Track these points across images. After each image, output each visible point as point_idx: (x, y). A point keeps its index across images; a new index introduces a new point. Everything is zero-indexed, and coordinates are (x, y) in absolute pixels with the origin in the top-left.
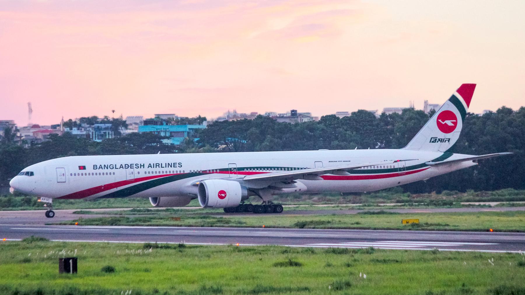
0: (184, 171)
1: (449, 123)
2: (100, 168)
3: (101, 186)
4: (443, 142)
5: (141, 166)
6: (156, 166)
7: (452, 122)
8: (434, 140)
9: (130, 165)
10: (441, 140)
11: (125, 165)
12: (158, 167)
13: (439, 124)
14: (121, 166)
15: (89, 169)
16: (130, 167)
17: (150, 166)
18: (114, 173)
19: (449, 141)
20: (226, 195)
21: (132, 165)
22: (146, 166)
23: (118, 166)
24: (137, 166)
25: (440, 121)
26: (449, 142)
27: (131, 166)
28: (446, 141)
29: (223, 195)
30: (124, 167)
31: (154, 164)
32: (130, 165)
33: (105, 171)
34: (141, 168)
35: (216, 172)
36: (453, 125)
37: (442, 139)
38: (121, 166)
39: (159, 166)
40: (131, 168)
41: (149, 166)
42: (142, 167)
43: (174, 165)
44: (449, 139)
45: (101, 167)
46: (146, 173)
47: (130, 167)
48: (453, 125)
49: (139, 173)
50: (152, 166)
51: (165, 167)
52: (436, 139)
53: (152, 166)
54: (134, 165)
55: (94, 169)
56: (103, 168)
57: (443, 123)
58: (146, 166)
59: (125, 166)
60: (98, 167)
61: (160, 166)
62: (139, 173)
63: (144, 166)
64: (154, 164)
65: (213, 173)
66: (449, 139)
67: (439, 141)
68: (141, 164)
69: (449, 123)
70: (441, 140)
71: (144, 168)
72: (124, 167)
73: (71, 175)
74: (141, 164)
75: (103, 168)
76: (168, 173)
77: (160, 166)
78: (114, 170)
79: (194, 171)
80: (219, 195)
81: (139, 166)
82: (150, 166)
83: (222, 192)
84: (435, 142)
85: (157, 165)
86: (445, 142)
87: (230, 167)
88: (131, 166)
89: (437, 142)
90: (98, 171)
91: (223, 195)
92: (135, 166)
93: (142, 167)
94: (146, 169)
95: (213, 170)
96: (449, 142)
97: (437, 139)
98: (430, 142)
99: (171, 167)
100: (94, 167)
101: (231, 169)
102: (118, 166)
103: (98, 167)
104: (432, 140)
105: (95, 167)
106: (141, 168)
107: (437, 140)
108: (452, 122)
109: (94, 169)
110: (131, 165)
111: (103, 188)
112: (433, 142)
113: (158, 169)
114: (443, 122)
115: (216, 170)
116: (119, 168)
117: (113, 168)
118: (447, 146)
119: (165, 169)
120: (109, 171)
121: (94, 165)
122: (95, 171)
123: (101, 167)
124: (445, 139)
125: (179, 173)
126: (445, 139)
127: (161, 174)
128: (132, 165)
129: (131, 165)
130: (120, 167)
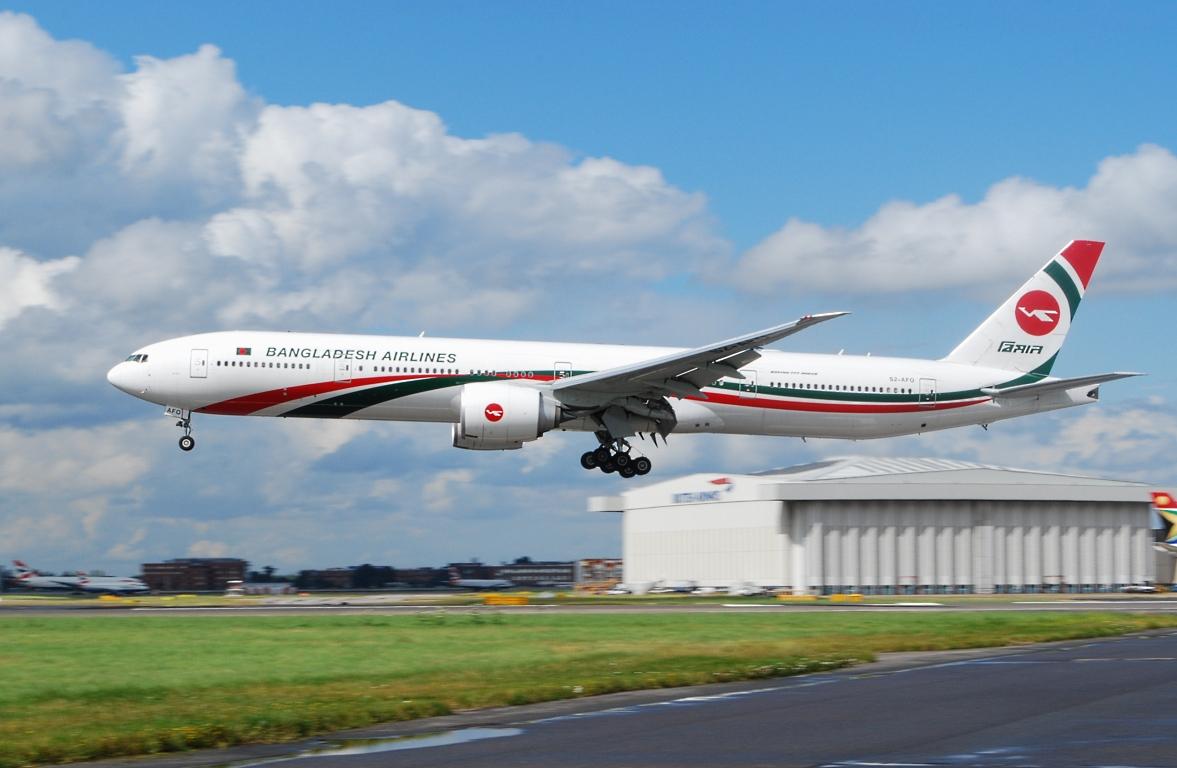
1: (1042, 315)
3: (281, 391)
7: (1048, 314)
8: (1008, 347)
10: (1024, 349)
12: (403, 359)
13: (1020, 316)
14: (327, 353)
17: (387, 356)
22: (379, 356)
24: (360, 355)
25: (1023, 309)
30: (332, 354)
32: (345, 352)
33: (291, 360)
35: (527, 378)
36: (1051, 320)
37: (1025, 347)
44: (1041, 348)
45: (283, 352)
46: (376, 369)
48: (1051, 320)
49: (361, 368)
50: (392, 357)
52: (1012, 346)
53: (392, 358)
57: (1030, 315)
58: (379, 356)
60: (277, 352)
61: (409, 357)
62: (361, 368)
65: (520, 377)
69: (1042, 315)
70: (1024, 349)
72: (332, 355)
73: (219, 363)
75: (288, 354)
76: (424, 373)
77: (409, 357)
81: (365, 355)
85: (403, 355)
87: (557, 369)
88: (347, 354)
89: (1015, 351)
90: (275, 360)
93: (370, 357)
94: (378, 362)
103: (277, 352)
104: (1004, 347)
105: (271, 352)
107: (1015, 347)
108: (1048, 314)
111: (285, 394)
112: (1005, 350)
114: (1030, 311)
118: (1038, 360)
119: (417, 365)
123: (283, 352)
125: (446, 373)
127: (409, 373)
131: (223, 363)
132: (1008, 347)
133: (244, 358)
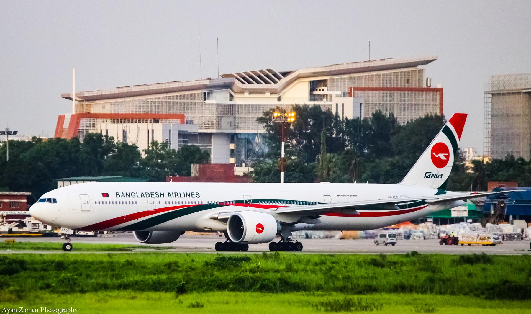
0: (202, 202)
2: (122, 196)
4: (436, 178)
5: (161, 195)
6: (175, 195)
8: (428, 175)
9: (150, 194)
10: (435, 176)
11: (146, 193)
14: (142, 195)
15: (112, 197)
16: (150, 196)
18: (136, 203)
19: (441, 176)
20: (263, 229)
21: (152, 194)
23: (139, 195)
26: (441, 178)
27: (151, 194)
28: (439, 176)
29: (261, 229)
31: (173, 193)
32: (150, 194)
33: (128, 199)
34: (161, 197)
37: (435, 174)
38: (142, 195)
39: (177, 195)
40: (152, 197)
41: (168, 196)
42: (162, 196)
43: (192, 195)
44: (442, 174)
45: (123, 195)
47: (150, 196)
51: (184, 196)
52: (430, 174)
54: (154, 194)
55: (117, 197)
56: (125, 196)
58: (166, 195)
59: (146, 195)
60: (121, 195)
61: (179, 195)
63: (163, 195)
64: (173, 193)
66: (442, 174)
67: (433, 176)
68: (160, 193)
70: (435, 176)
71: (164, 197)
73: (96, 203)
74: (160, 193)
75: (125, 196)
77: (179, 195)
78: (136, 199)
79: (211, 202)
80: (256, 229)
82: (169, 195)
83: (260, 225)
84: (429, 177)
85: (176, 195)
86: (438, 178)
88: (151, 195)
89: (431, 177)
91: (261, 229)
92: (155, 195)
93: (162, 196)
95: (229, 202)
96: (441, 178)
97: (431, 173)
98: (425, 177)
99: (190, 197)
100: (117, 195)
101: (246, 201)
102: (139, 195)
103: (121, 195)
104: (427, 175)
105: (117, 195)
106: (161, 197)
109: (117, 197)
110: (151, 193)
112: (427, 177)
113: (177, 199)
115: (232, 201)
116: (140, 196)
117: (135, 197)
118: (440, 182)
120: (131, 199)
121: (116, 193)
122: (118, 200)
124: (438, 175)
126: (438, 175)
128: (152, 194)
129: (151, 193)
130: (142, 196)
131: (97, 203)
132: (428, 175)
133: (106, 199)
